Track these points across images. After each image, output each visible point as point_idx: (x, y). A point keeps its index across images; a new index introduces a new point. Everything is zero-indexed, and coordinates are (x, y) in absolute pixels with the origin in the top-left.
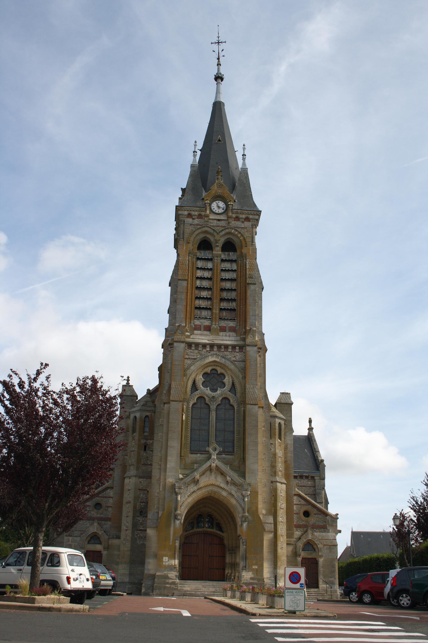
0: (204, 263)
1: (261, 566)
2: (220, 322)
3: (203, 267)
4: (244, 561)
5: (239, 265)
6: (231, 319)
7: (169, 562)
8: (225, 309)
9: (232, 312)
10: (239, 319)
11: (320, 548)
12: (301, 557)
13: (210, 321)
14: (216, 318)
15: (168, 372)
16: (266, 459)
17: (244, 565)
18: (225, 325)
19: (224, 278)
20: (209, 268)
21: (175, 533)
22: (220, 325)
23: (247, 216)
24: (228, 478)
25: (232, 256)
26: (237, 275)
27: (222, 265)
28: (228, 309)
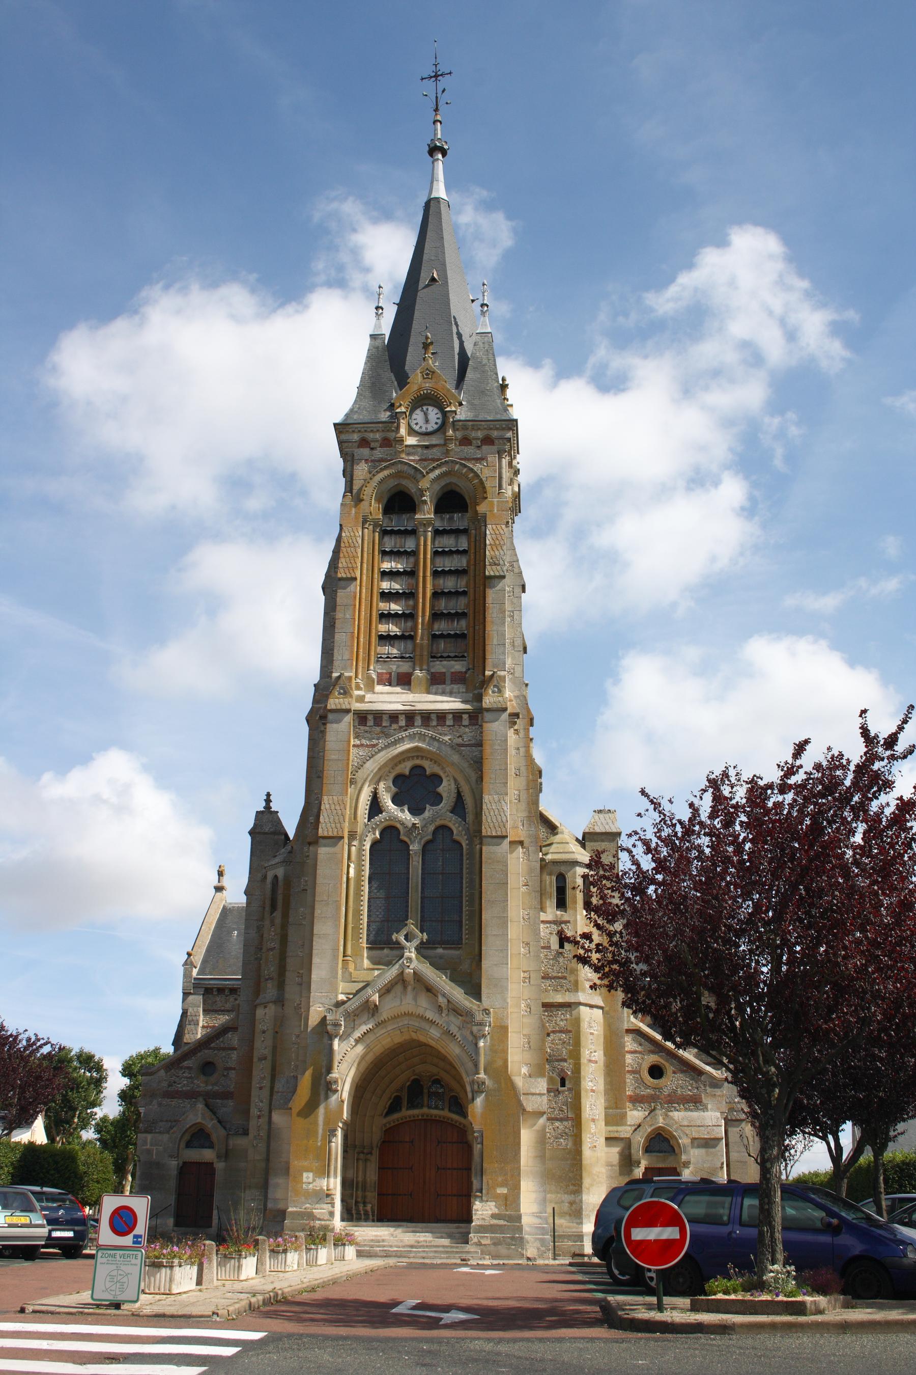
0: (398, 540)
2: (432, 664)
3: (396, 550)
5: (473, 539)
6: (456, 657)
8: (442, 636)
9: (459, 640)
10: (471, 655)
13: (410, 664)
14: (421, 655)
18: (444, 670)
19: (440, 569)
20: (409, 550)
22: (433, 670)
23: (486, 432)
25: (459, 520)
26: (468, 562)
27: (437, 542)
28: (449, 636)
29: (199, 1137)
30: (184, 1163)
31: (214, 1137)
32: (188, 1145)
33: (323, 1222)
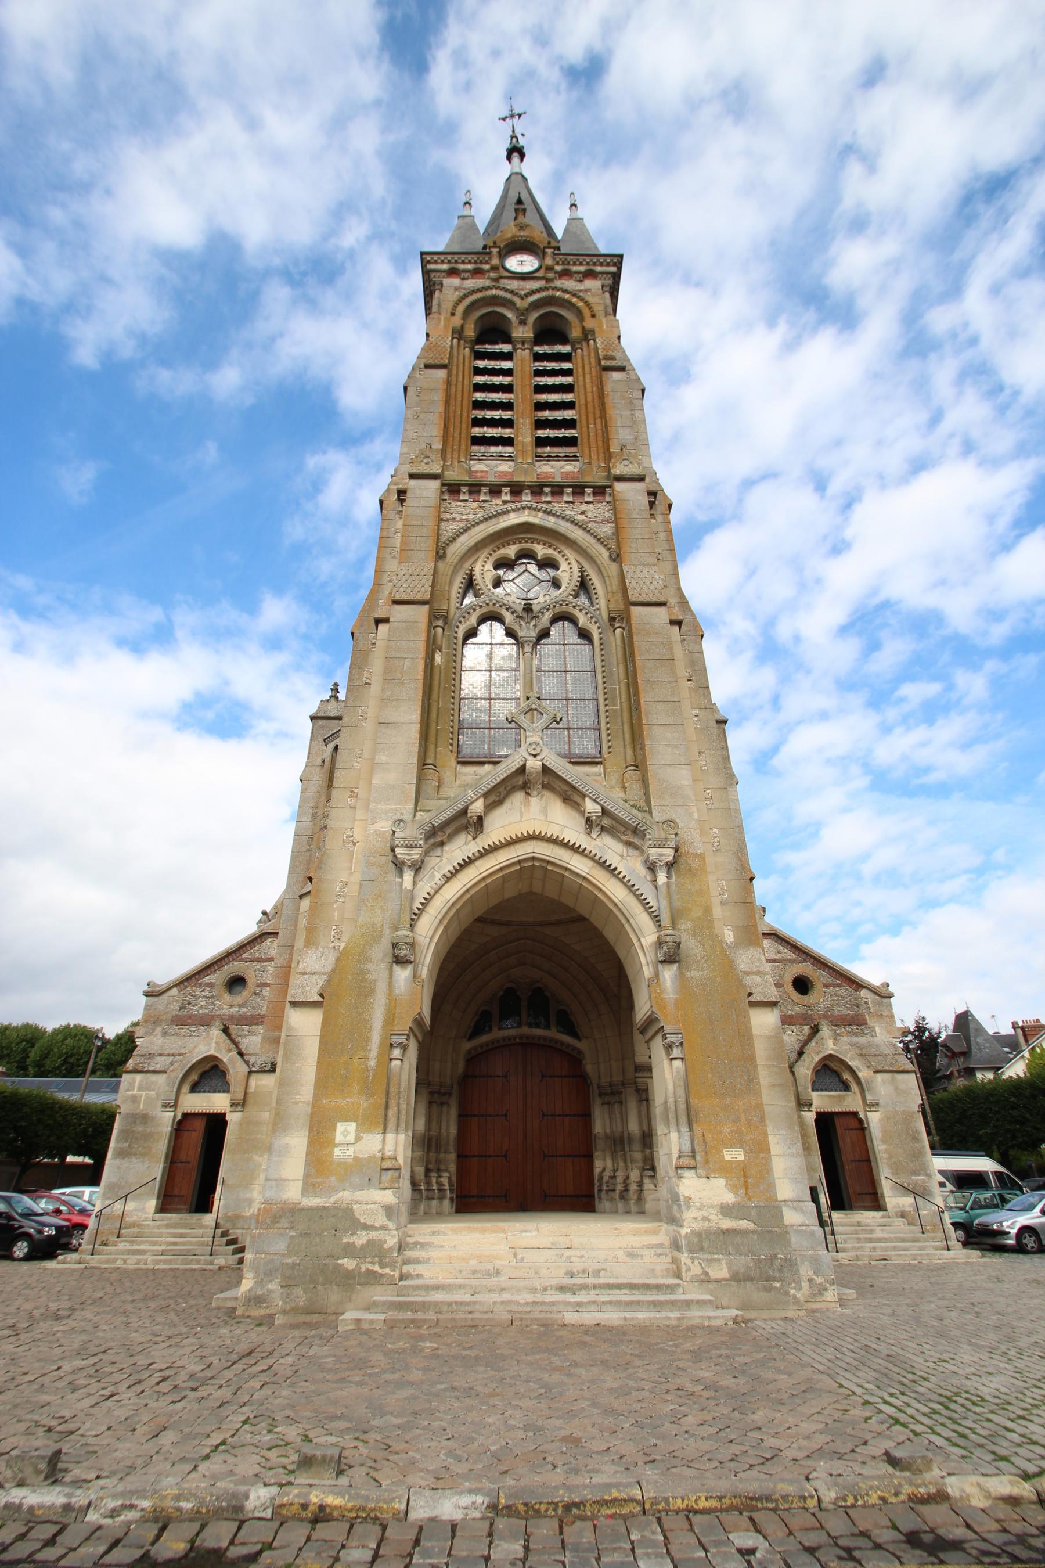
1: (760, 1149)
4: (684, 1129)
7: (358, 1146)
11: (867, 1082)
12: (813, 1108)
15: (394, 557)
16: (710, 766)
17: (687, 1147)
21: (390, 1019)
24: (590, 807)
29: (209, 1074)
30: (185, 1115)
31: (231, 1078)
32: (194, 1088)
33: (373, 1235)
